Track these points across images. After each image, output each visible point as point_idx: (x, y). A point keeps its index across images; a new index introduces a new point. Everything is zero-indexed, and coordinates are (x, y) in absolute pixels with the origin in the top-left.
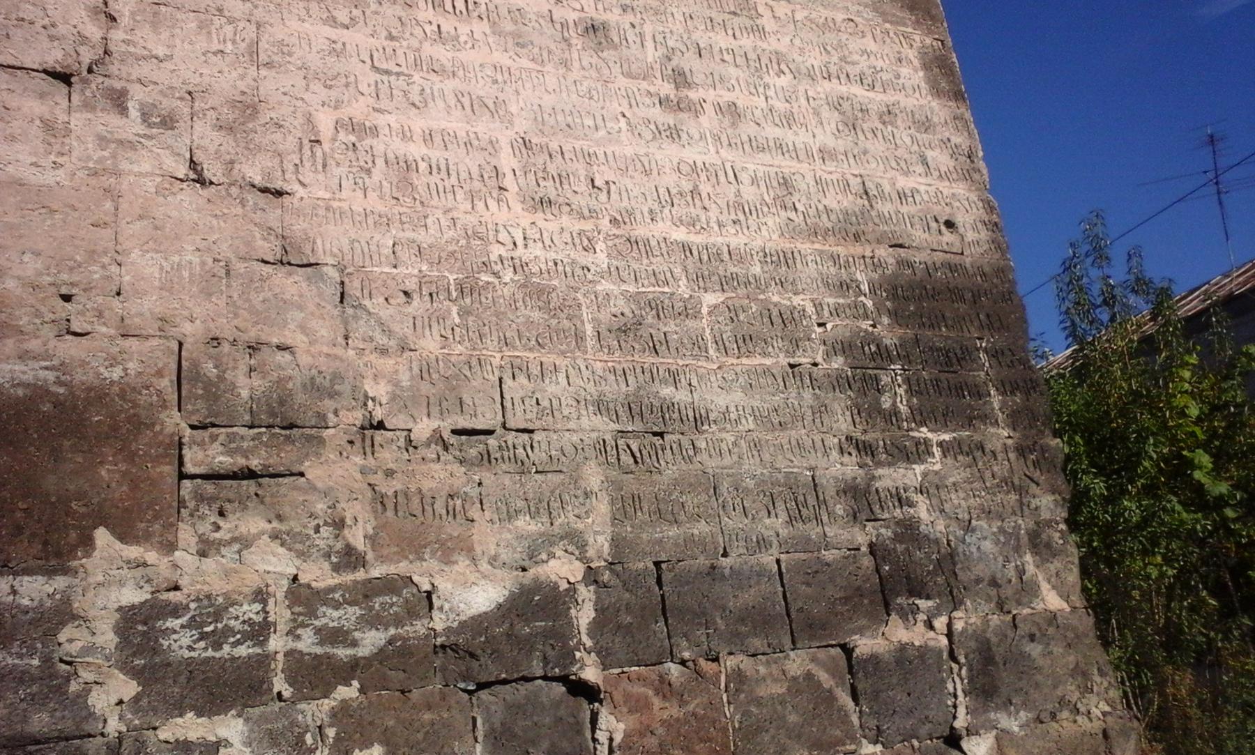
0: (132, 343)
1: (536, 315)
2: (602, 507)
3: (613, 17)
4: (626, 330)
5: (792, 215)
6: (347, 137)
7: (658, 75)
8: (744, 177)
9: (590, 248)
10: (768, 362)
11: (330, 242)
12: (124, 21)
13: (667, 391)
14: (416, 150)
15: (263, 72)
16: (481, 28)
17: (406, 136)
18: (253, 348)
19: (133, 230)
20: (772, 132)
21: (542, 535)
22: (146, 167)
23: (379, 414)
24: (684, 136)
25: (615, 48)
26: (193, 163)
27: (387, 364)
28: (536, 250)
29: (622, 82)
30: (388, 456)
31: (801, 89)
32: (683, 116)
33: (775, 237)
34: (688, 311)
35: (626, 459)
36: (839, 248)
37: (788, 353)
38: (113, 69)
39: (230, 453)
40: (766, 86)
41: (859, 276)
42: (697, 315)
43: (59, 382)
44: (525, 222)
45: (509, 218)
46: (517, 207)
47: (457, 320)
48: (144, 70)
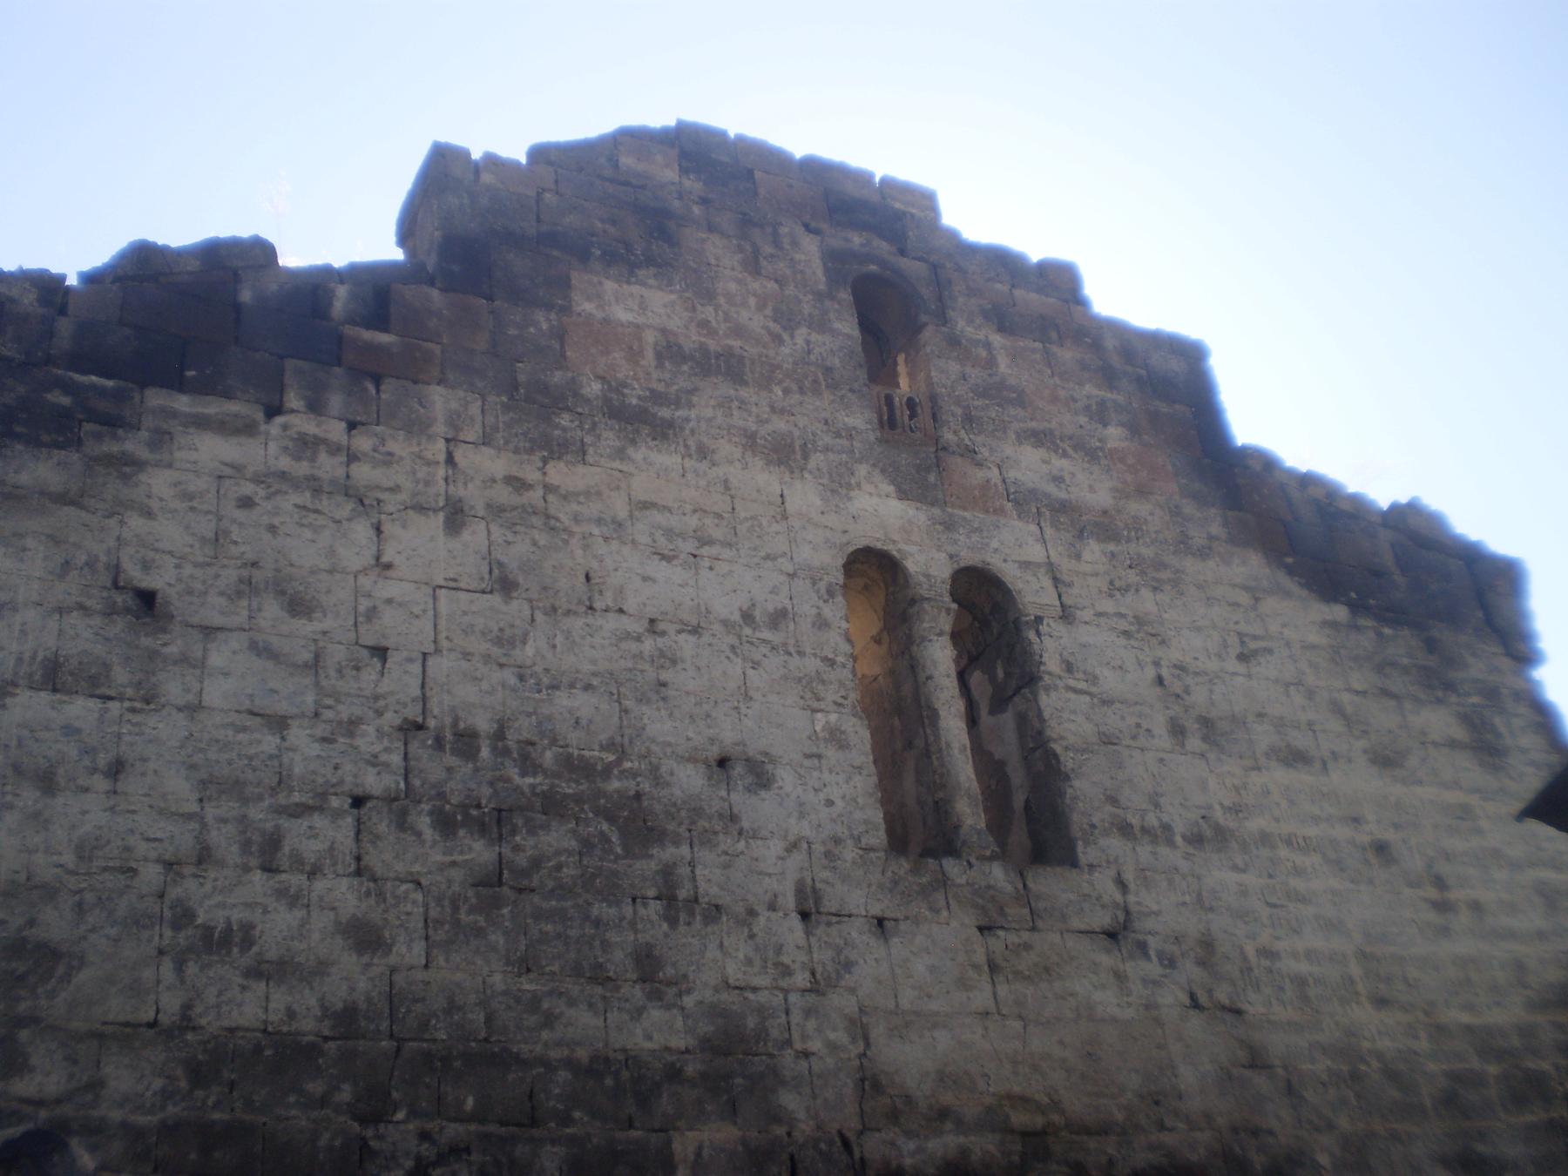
0: (1198, 1135)
3: (1390, 836)
11: (1277, 1044)
12: (1132, 886)
14: (1303, 967)
15: (1210, 916)
16: (1316, 859)
17: (1295, 955)
22: (1169, 1000)
26: (1192, 996)
38: (1137, 925)
45: (1363, 1015)
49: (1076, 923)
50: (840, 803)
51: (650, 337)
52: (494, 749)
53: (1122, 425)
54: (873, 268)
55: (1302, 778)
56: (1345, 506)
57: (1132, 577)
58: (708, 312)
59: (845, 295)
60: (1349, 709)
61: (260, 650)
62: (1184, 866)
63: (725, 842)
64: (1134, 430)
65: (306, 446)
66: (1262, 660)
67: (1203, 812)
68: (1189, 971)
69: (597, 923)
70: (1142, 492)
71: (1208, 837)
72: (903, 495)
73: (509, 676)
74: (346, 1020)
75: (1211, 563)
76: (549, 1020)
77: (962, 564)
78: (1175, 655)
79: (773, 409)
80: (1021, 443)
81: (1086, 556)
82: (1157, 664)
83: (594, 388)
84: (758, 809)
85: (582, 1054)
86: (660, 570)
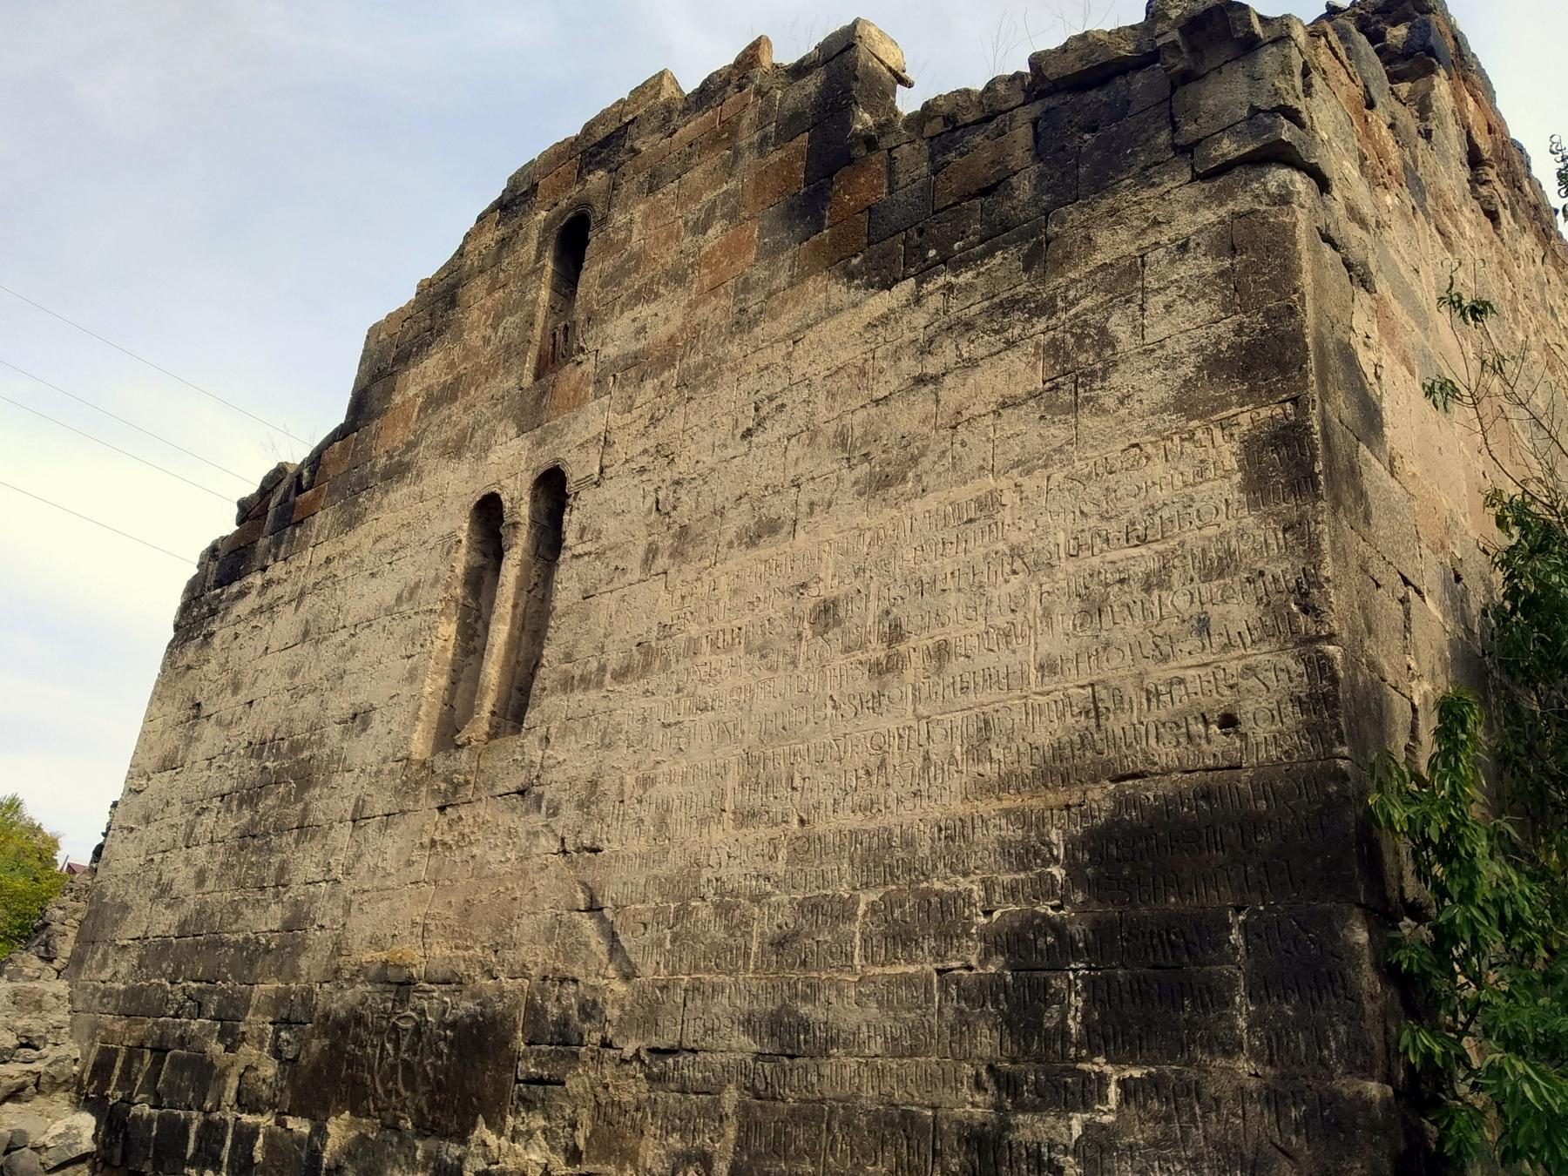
1: (721, 934)
2: (731, 1133)
4: (780, 943)
5: (987, 769)
6: (639, 792)
7: (873, 638)
8: (938, 733)
13: (804, 1010)
14: (674, 790)
18: (563, 980)
20: (983, 660)
21: (683, 1154)
23: (610, 1032)
24: (885, 701)
25: (838, 623)
29: (839, 660)
30: (608, 1070)
32: (889, 676)
34: (846, 911)
36: (1034, 802)
37: (939, 956)
39: (535, 1066)
40: (989, 602)
41: (1054, 838)
42: (850, 916)
43: (482, 1014)
47: (668, 946)
48: (555, 775)
49: (500, 790)
52: (271, 749)
53: (723, 217)
55: (766, 549)
57: (673, 396)
58: (457, 352)
61: (219, 723)
62: (601, 706)
63: (337, 779)
64: (732, 216)
65: (268, 584)
66: (768, 424)
67: (638, 640)
68: (569, 814)
69: (271, 851)
70: (713, 290)
72: (521, 431)
73: (287, 697)
74: (183, 925)
76: (239, 914)
77: (541, 471)
80: (622, 312)
84: (365, 751)
85: (241, 937)
86: (374, 583)
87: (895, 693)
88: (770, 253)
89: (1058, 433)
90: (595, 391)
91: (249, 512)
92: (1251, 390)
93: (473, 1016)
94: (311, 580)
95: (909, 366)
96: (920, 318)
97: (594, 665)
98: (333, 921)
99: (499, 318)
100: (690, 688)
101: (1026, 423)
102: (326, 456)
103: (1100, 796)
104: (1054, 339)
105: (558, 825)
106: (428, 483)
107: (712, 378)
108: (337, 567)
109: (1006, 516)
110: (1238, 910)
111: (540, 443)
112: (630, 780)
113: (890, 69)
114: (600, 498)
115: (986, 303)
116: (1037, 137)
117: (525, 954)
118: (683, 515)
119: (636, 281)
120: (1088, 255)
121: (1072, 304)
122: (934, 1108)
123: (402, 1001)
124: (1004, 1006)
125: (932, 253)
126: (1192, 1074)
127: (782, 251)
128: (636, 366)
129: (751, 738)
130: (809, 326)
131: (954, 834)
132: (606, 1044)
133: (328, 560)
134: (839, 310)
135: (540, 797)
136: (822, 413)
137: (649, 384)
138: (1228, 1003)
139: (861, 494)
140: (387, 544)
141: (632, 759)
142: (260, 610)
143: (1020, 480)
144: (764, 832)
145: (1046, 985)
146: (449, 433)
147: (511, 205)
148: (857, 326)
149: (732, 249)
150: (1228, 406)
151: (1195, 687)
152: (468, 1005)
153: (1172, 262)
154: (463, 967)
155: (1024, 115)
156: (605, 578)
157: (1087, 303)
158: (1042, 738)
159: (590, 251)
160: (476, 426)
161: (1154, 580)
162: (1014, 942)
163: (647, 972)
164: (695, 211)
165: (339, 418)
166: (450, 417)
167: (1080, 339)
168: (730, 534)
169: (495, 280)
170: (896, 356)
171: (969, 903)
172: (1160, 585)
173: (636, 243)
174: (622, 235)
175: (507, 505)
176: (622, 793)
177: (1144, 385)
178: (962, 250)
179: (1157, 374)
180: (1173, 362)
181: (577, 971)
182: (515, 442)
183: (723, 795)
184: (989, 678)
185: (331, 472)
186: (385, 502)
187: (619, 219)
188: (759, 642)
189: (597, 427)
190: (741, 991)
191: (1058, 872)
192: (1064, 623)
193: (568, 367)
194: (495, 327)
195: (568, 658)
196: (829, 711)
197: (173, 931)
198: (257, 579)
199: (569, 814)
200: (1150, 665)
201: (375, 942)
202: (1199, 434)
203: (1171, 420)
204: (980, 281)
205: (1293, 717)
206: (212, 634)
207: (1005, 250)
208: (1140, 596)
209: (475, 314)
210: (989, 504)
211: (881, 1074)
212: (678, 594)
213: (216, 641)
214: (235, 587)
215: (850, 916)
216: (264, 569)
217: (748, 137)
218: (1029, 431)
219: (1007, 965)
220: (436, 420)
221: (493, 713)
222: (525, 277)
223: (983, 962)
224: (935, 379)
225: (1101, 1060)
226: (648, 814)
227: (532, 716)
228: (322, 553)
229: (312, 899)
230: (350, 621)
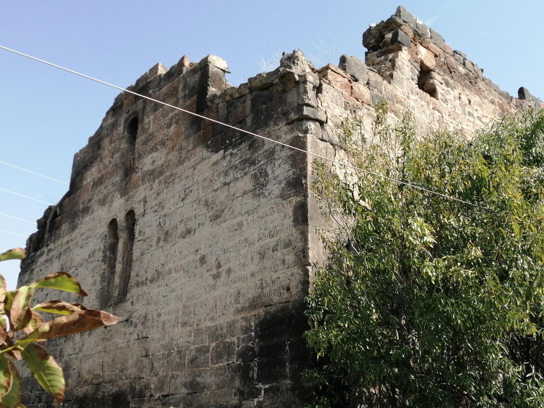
3: (206, 253)
4: (192, 361)
6: (157, 318)
9: (190, 336)
10: (221, 365)
13: (198, 379)
19: (130, 354)
20: (239, 273)
27: (155, 379)
28: (182, 340)
29: (206, 274)
31: (250, 250)
33: (232, 316)
35: (188, 402)
37: (228, 360)
44: (180, 332)
46: (180, 327)
50: (91, 301)
51: (91, 183)
53: (175, 123)
54: (133, 117)
55: (187, 240)
56: (236, 96)
59: (125, 134)
60: (210, 201)
62: (147, 291)
64: (177, 123)
65: (50, 251)
66: (188, 197)
68: (140, 327)
71: (158, 276)
72: (122, 196)
75: (185, 164)
77: (128, 211)
78: (166, 210)
79: (105, 188)
81: (154, 188)
82: (160, 218)
83: (81, 206)
86: (82, 250)
87: (219, 284)
88: (187, 137)
89: (256, 203)
90: (142, 183)
91: (41, 224)
92: (296, 192)
93: (117, 392)
94: (62, 250)
95: (222, 179)
96: (225, 163)
97: (144, 278)
98: (77, 366)
99: (113, 154)
100: (169, 284)
101: (249, 199)
102: (64, 203)
103: (261, 311)
104: (255, 173)
105: (136, 330)
106: (96, 214)
107: (173, 180)
108: (70, 244)
109: (244, 228)
110: (288, 341)
111: (127, 200)
112: (155, 315)
113: (222, 70)
114: (145, 221)
115: (240, 160)
116: (252, 105)
117: (129, 371)
118: (167, 227)
119: (151, 144)
120: (263, 146)
121: (259, 162)
122: (227, 402)
123: (97, 390)
124: (241, 373)
125: (228, 142)
126: (278, 385)
127: (191, 137)
128: (153, 175)
129: (184, 300)
130: (198, 164)
131: (231, 325)
132: (151, 396)
133: (68, 242)
134: (205, 159)
135: (132, 322)
136: (202, 194)
137: (157, 181)
138: (285, 366)
139: (211, 221)
140: (84, 236)
141: (156, 307)
142: (46, 261)
143: (247, 217)
144: (188, 328)
145: (250, 365)
146: (101, 196)
147: (116, 110)
148: (210, 165)
149: (177, 134)
150: (291, 197)
151: (277, 281)
152: (115, 389)
153: (281, 151)
154: (114, 377)
155: (249, 97)
156: (147, 248)
157: (262, 162)
158: (250, 296)
159: (139, 131)
160: (109, 194)
161: (275, 248)
162: (242, 355)
163: (161, 373)
164: (167, 120)
165: (67, 189)
166: (101, 190)
167: (261, 173)
168: (179, 234)
169: (111, 139)
170: (219, 176)
171: (234, 345)
172: (277, 250)
173: (151, 131)
174: (147, 126)
175: (119, 222)
176: (153, 319)
177: (274, 188)
178: (235, 141)
179: (277, 186)
180: (280, 182)
181: (143, 375)
182: (120, 200)
183: (178, 318)
184: (240, 279)
185: (66, 210)
186: (83, 221)
187: (146, 121)
188: (186, 269)
189: (142, 196)
190: (183, 377)
191: (253, 334)
192: (256, 261)
193: (134, 174)
194: (112, 157)
195: (138, 275)
196: (203, 290)
197: (30, 375)
198: (45, 249)
199: (140, 327)
200: (272, 273)
201: (89, 372)
202: (285, 205)
203: (279, 200)
204: (239, 152)
205: (300, 287)
206: (33, 270)
207: (245, 142)
208: (271, 253)
209: (106, 152)
210: (240, 225)
211: (215, 395)
212: (165, 254)
213: (35, 272)
214: (39, 253)
215: (208, 351)
216: (48, 246)
217: (181, 94)
218: (249, 202)
219: (242, 361)
220: (97, 191)
221: (119, 294)
222: (120, 139)
223: (237, 361)
224: (229, 184)
225: (260, 384)
226: (160, 325)
227: (129, 295)
228: (65, 239)
229: (71, 360)
230: (75, 264)
